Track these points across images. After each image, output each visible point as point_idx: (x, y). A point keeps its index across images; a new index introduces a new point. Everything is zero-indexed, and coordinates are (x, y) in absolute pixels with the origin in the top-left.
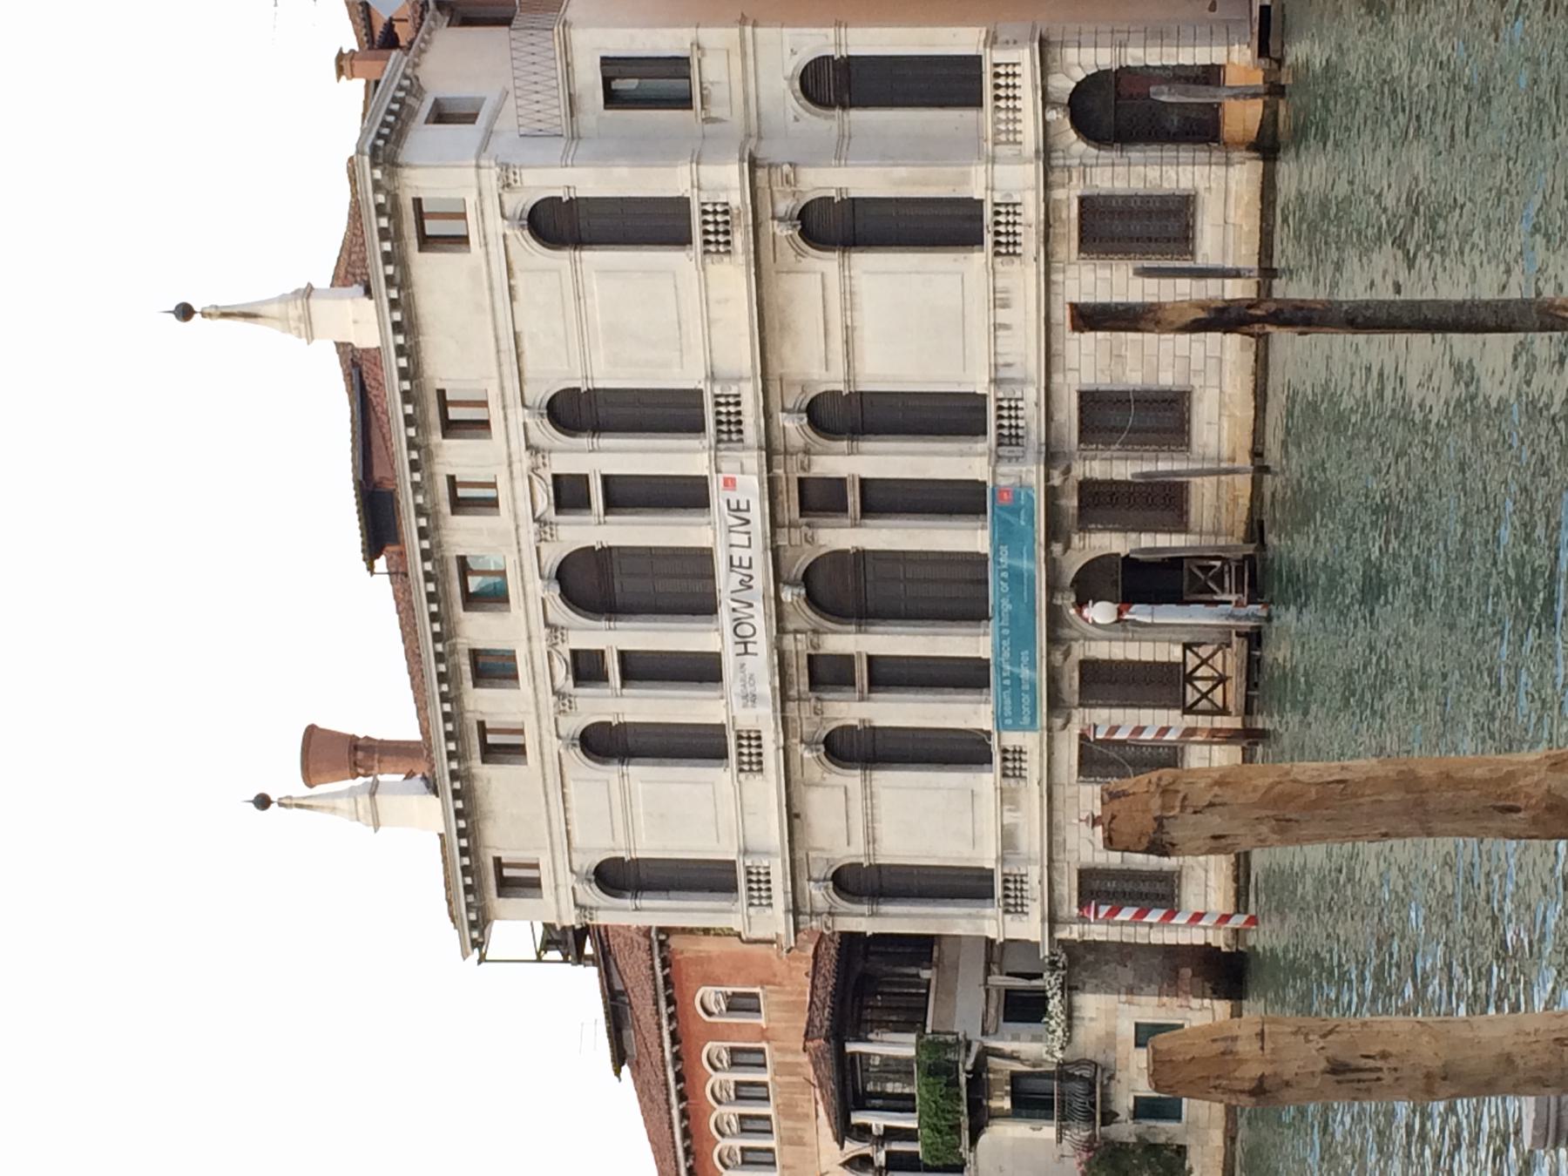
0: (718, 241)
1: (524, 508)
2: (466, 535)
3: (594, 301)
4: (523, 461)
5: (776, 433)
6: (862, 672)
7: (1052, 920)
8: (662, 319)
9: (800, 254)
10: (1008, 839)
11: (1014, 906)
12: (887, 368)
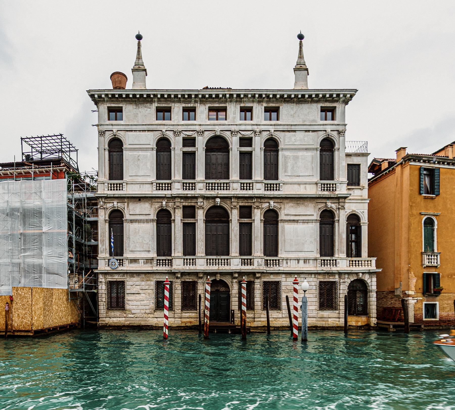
3: (305, 153)
5: (266, 201)
7: (105, 274)
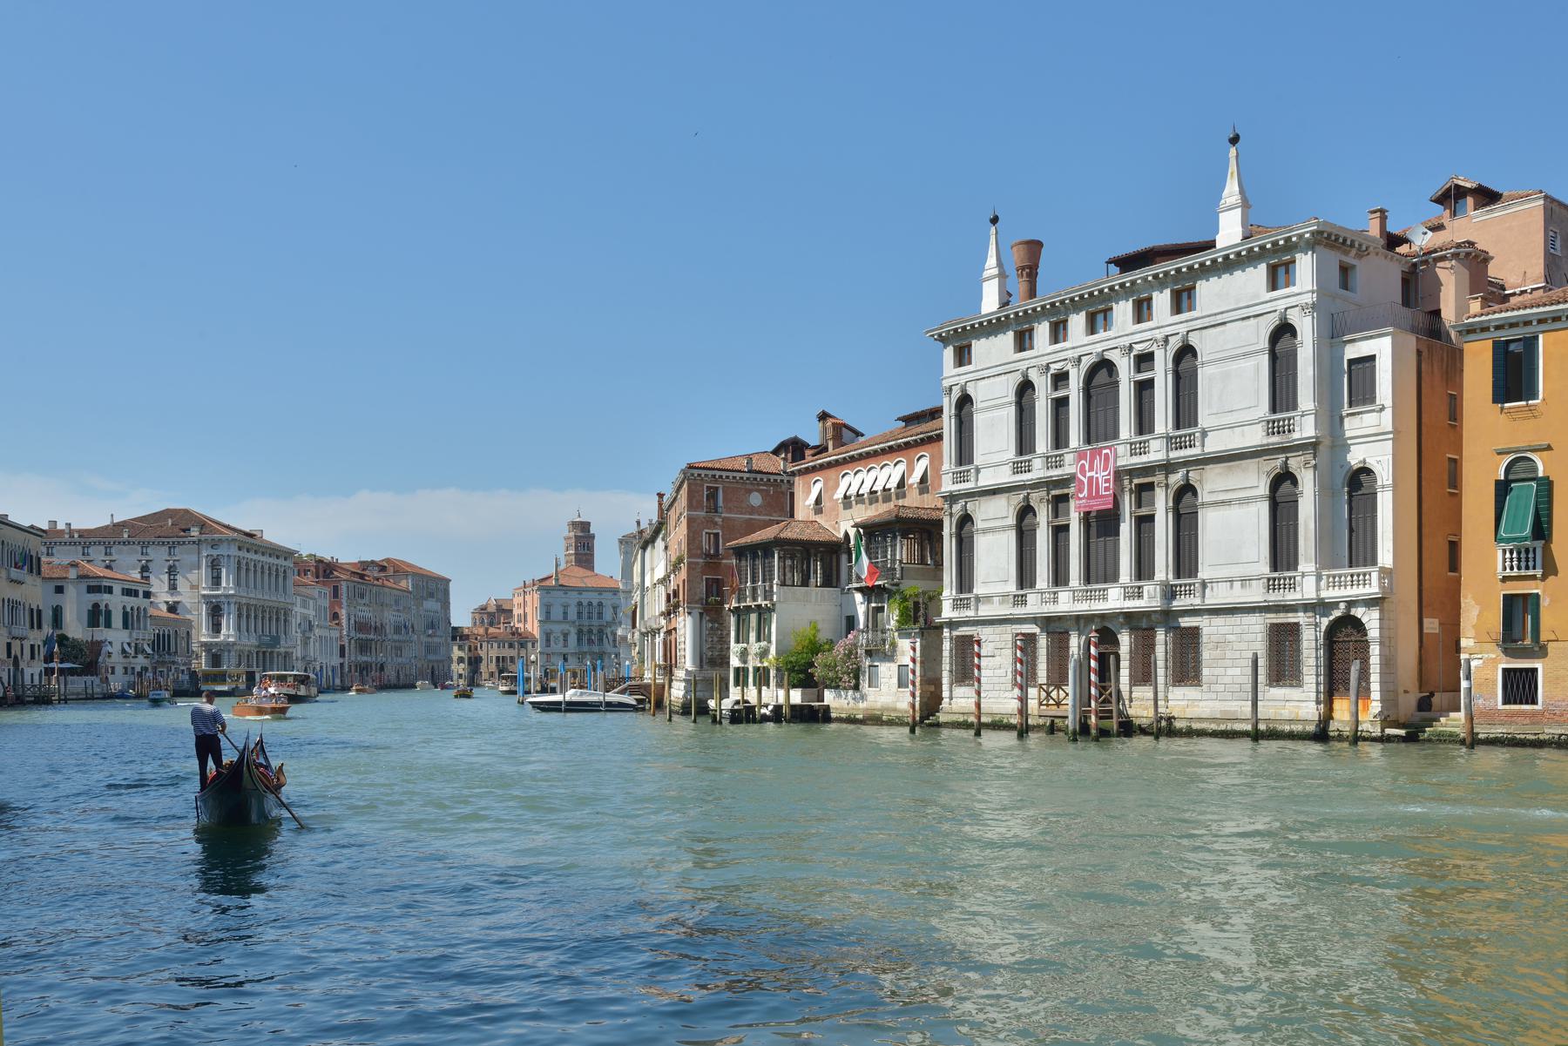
0: (1273, 428)
1: (1137, 338)
2: (1123, 311)
4: (1159, 334)
6: (1061, 521)
8: (1234, 403)
9: (1268, 474)
10: (988, 598)
11: (958, 604)
12: (1211, 524)
